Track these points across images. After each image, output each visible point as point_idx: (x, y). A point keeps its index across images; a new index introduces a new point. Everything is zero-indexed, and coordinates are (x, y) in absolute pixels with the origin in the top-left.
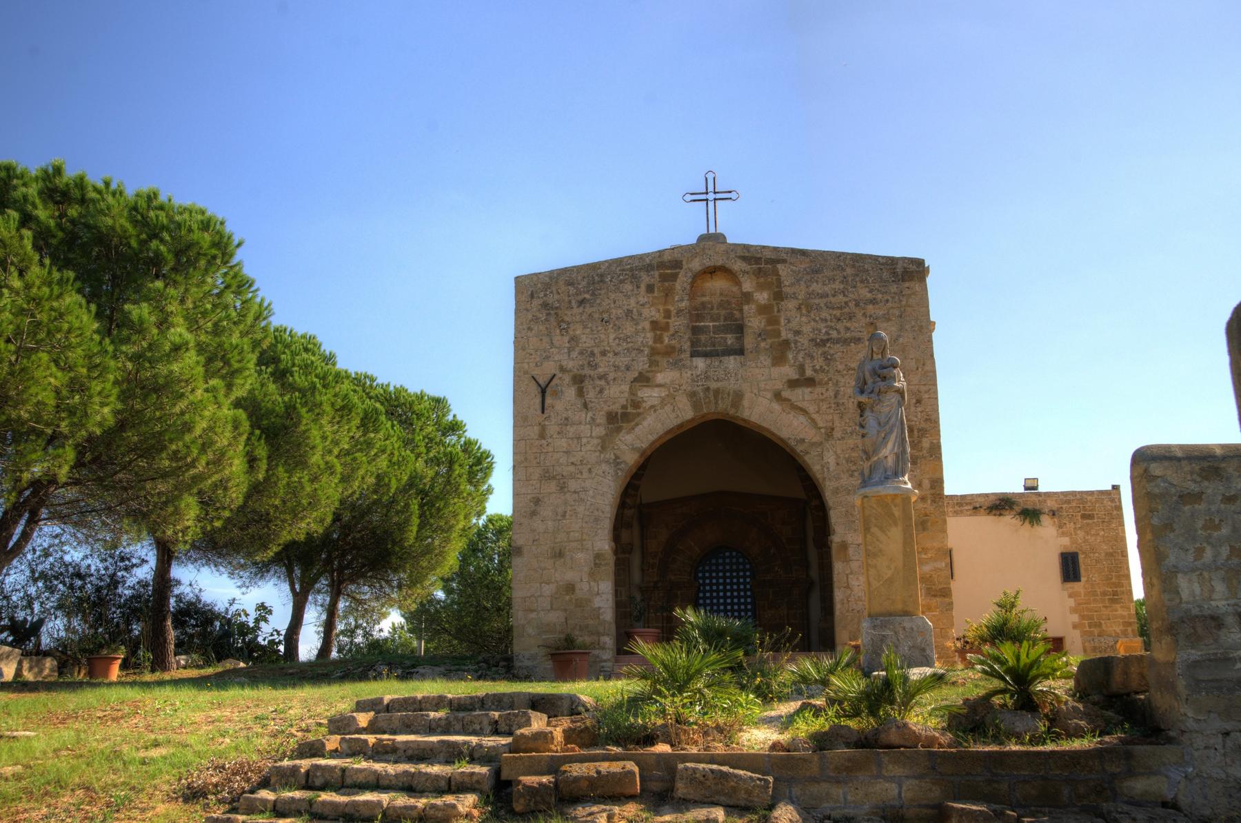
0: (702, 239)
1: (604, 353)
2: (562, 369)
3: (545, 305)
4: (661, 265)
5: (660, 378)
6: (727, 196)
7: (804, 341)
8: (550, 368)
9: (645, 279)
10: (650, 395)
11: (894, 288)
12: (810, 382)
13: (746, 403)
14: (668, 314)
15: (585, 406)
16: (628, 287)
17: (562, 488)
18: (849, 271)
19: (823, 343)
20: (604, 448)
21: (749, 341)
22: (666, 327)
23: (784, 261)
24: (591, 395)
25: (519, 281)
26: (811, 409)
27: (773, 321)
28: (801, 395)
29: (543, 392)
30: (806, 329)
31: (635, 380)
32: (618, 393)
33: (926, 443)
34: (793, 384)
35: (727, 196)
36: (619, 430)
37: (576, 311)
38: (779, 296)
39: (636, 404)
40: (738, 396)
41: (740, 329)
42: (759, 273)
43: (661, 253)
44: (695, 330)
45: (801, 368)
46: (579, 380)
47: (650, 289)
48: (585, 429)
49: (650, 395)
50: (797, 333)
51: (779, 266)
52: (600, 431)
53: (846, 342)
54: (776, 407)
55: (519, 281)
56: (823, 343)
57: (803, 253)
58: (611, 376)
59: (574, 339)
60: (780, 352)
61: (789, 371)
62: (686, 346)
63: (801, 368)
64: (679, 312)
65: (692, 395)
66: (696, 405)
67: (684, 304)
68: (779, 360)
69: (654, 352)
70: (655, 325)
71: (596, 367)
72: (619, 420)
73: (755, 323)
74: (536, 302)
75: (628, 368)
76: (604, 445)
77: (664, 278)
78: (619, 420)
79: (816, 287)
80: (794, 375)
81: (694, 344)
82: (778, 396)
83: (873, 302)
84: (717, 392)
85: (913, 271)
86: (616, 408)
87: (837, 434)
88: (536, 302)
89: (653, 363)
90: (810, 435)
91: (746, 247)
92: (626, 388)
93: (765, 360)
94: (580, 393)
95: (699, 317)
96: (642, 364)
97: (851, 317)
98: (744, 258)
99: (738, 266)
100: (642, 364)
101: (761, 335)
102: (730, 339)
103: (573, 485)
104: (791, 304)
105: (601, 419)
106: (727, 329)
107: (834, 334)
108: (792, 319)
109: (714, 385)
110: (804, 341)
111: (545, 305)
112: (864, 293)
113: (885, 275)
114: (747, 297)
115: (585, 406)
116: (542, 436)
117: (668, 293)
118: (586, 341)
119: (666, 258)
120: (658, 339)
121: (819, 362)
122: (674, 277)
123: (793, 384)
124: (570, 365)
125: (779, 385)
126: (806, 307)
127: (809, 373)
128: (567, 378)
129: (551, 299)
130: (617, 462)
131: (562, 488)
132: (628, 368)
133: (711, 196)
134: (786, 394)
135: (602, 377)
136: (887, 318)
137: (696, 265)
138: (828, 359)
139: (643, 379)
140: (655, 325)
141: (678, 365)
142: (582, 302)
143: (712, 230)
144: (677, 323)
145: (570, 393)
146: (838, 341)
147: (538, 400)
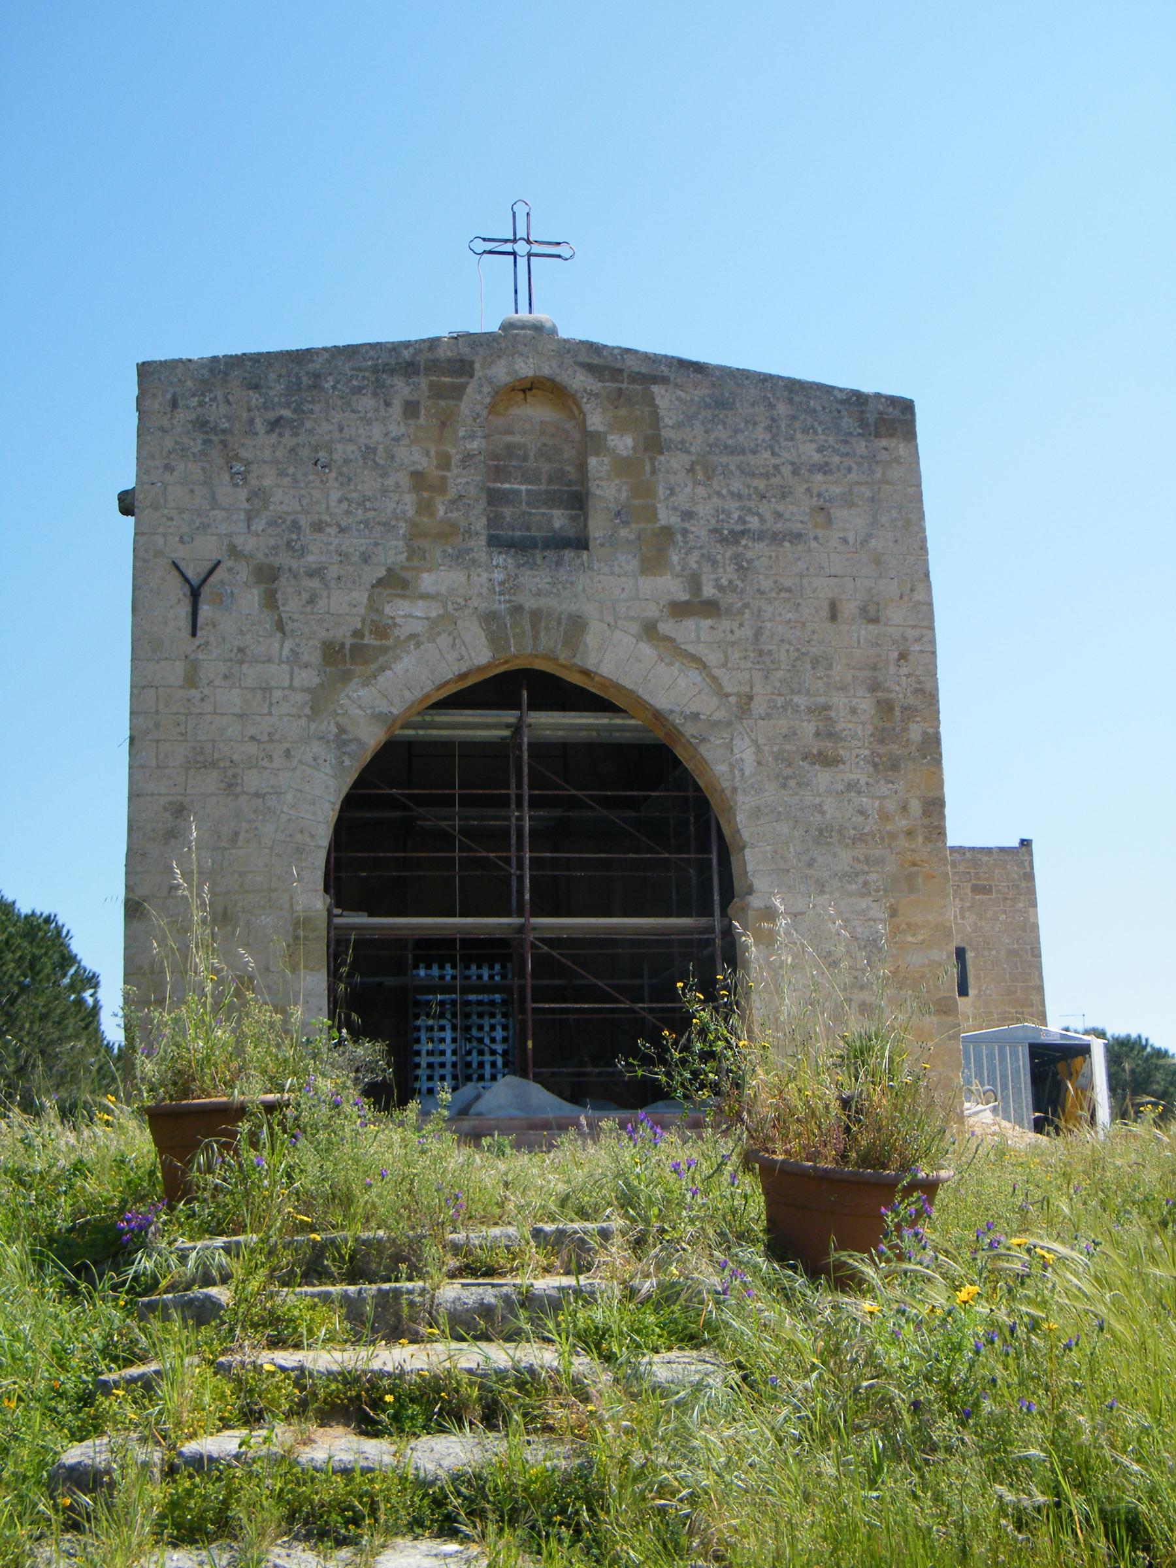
0: (507, 326)
1: (318, 527)
3: (201, 424)
4: (434, 367)
5: (428, 581)
6: (554, 250)
7: (699, 531)
8: (208, 548)
9: (402, 389)
11: (861, 446)
12: (710, 608)
13: (591, 640)
14: (444, 463)
15: (280, 626)
16: (367, 403)
17: (231, 787)
18: (782, 409)
19: (735, 537)
21: (597, 527)
22: (441, 487)
23: (663, 380)
24: (291, 605)
25: (147, 372)
26: (713, 658)
27: (644, 490)
29: (195, 595)
30: (704, 510)
31: (380, 582)
33: (915, 732)
34: (679, 610)
35: (554, 250)
36: (346, 677)
37: (265, 440)
38: (654, 444)
39: (382, 630)
40: (577, 625)
43: (434, 343)
44: (495, 498)
45: (695, 582)
46: (267, 576)
47: (411, 409)
50: (688, 515)
51: (655, 389)
52: (309, 677)
53: (776, 539)
55: (147, 372)
56: (735, 537)
57: (699, 368)
58: (333, 572)
59: (259, 496)
61: (670, 586)
62: (480, 524)
63: (695, 582)
64: (467, 458)
65: (489, 618)
66: (496, 639)
67: (474, 445)
68: (653, 563)
69: (416, 532)
71: (303, 552)
74: (183, 416)
75: (366, 559)
77: (438, 392)
79: (721, 433)
81: (494, 521)
82: (650, 630)
83: (824, 469)
86: (342, 633)
87: (759, 706)
88: (183, 416)
89: (413, 553)
90: (707, 705)
91: (593, 348)
92: (361, 596)
93: (628, 562)
94: (271, 600)
95: (500, 473)
96: (393, 553)
98: (590, 368)
99: (579, 381)
100: (393, 553)
101: (622, 514)
102: (559, 519)
103: (252, 780)
104: (676, 462)
105: (311, 654)
106: (551, 500)
107: (754, 523)
109: (529, 603)
110: (699, 531)
111: (201, 424)
112: (808, 451)
113: (847, 423)
114: (591, 442)
115: (280, 626)
116: (191, 680)
117: (445, 423)
118: (283, 501)
119: (442, 353)
120: (425, 508)
121: (728, 574)
122: (458, 392)
123: (679, 610)
124: (248, 544)
125: (653, 611)
127: (708, 591)
128: (244, 572)
129: (216, 412)
131: (231, 787)
132: (366, 559)
133: (522, 248)
134: (666, 627)
135: (316, 573)
137: (501, 373)
138: (743, 568)
140: (418, 477)
141: (460, 558)
142: (275, 424)
143: (523, 314)
144: (462, 481)
145: (251, 599)
146: (760, 536)
147: (184, 610)
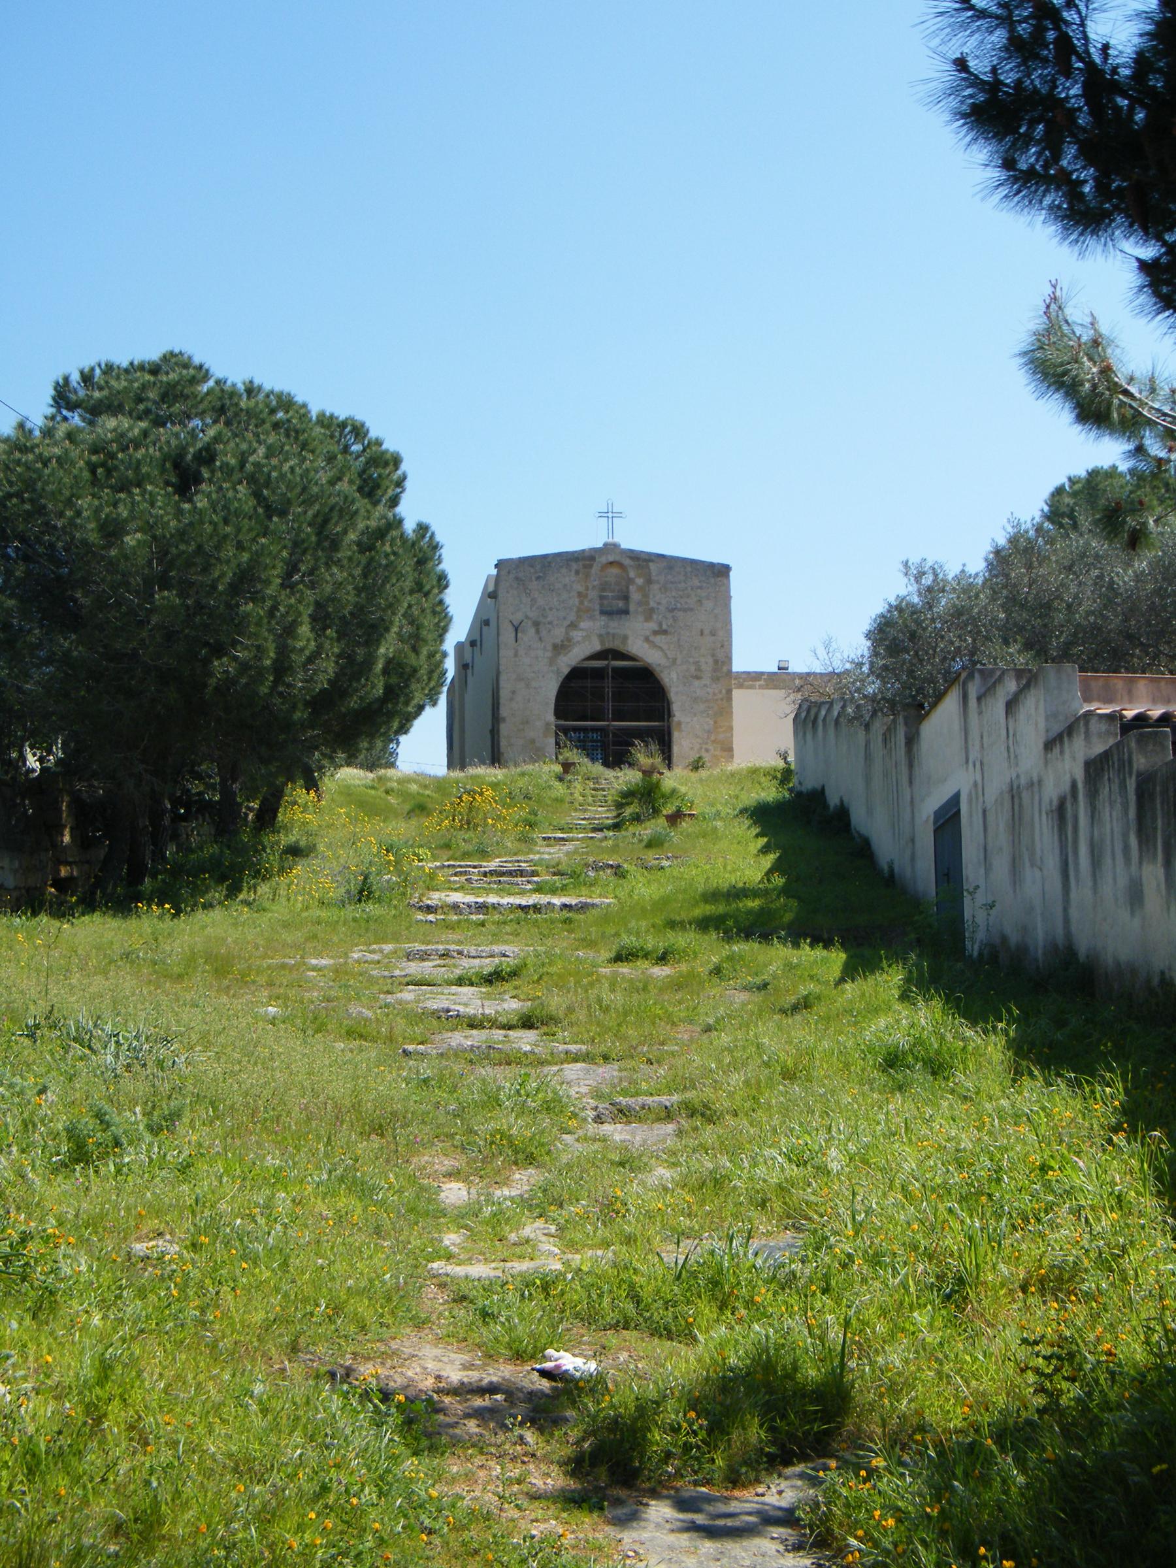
0: (606, 545)
1: (551, 609)
2: (527, 617)
3: (517, 578)
4: (584, 559)
5: (582, 625)
6: (619, 515)
7: (662, 608)
8: (519, 616)
9: (574, 566)
10: (577, 635)
11: (712, 580)
12: (665, 632)
13: (630, 642)
14: (587, 589)
15: (540, 639)
16: (564, 571)
17: (528, 686)
18: (689, 569)
19: (672, 610)
20: (551, 665)
21: (632, 608)
22: (586, 596)
23: (652, 561)
24: (544, 633)
26: (665, 647)
27: (646, 596)
28: (658, 639)
29: (516, 630)
30: (664, 602)
31: (569, 626)
32: (559, 633)
33: (725, 669)
34: (655, 633)
35: (619, 515)
36: (559, 654)
37: (535, 583)
38: (649, 581)
39: (569, 640)
40: (625, 638)
41: (626, 598)
42: (639, 567)
43: (583, 551)
44: (602, 598)
45: (660, 624)
46: (536, 624)
47: (577, 572)
48: (540, 653)
49: (577, 635)
50: (659, 603)
51: (651, 564)
52: (549, 654)
53: (685, 610)
54: (646, 645)
56: (672, 610)
57: (663, 556)
58: (555, 622)
59: (534, 600)
60: (649, 614)
61: (653, 625)
62: (597, 607)
63: (660, 624)
64: (594, 587)
65: (600, 636)
66: (602, 643)
67: (596, 583)
68: (648, 618)
69: (579, 610)
70: (580, 594)
71: (545, 617)
72: (560, 648)
73: (635, 596)
74: (512, 576)
75: (565, 618)
76: (552, 662)
77: (585, 567)
78: (560, 648)
79: (669, 577)
80: (656, 628)
81: (601, 605)
82: (647, 639)
83: (700, 588)
84: (614, 635)
85: (721, 572)
86: (558, 641)
87: (679, 662)
88: (512, 576)
89: (579, 617)
90: (663, 662)
91: (631, 551)
92: (563, 630)
93: (641, 618)
94: (538, 632)
95: (603, 590)
96: (572, 617)
97: (689, 596)
98: (631, 558)
99: (627, 562)
100: (572, 617)
101: (639, 604)
102: (621, 604)
103: (534, 684)
104: (655, 587)
105: (550, 648)
106: (618, 598)
107: (679, 605)
108: (657, 597)
109: (612, 631)
110: (662, 608)
111: (517, 578)
112: (696, 582)
113: (709, 573)
114: (630, 581)
115: (540, 639)
116: (516, 655)
117: (587, 576)
118: (541, 602)
119: (587, 554)
120: (581, 603)
121: (671, 621)
122: (591, 566)
123: (655, 633)
124: (531, 614)
125: (648, 633)
126: (664, 589)
127: (664, 627)
128: (530, 623)
129: (521, 575)
130: (558, 672)
131: (528, 686)
132: (565, 618)
133: (610, 515)
134: (652, 638)
135: (550, 623)
136: (708, 598)
137: (603, 560)
138: (675, 619)
139: (573, 626)
140: (580, 594)
141: (592, 618)
142: (538, 578)
143: (610, 540)
144: (593, 594)
145: (532, 631)
146: (680, 610)
147: (513, 634)
